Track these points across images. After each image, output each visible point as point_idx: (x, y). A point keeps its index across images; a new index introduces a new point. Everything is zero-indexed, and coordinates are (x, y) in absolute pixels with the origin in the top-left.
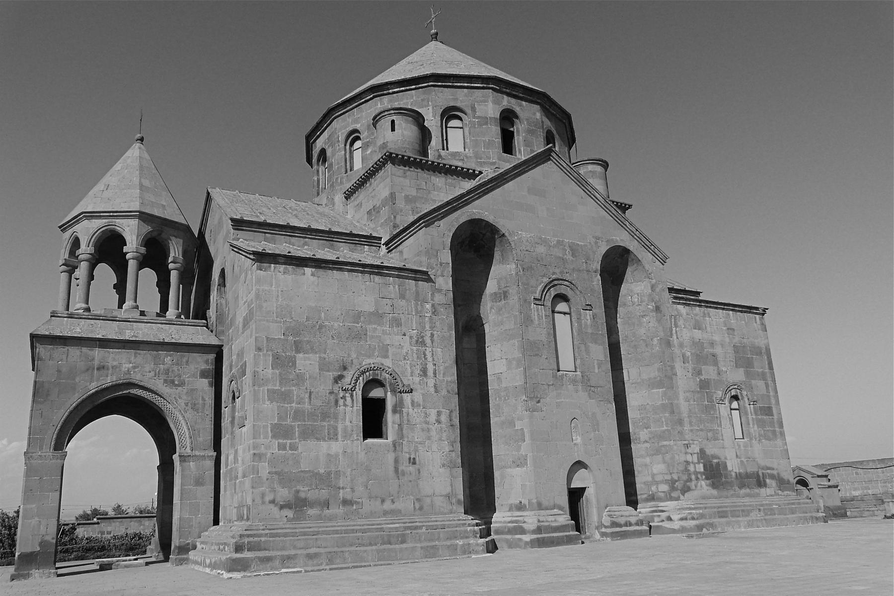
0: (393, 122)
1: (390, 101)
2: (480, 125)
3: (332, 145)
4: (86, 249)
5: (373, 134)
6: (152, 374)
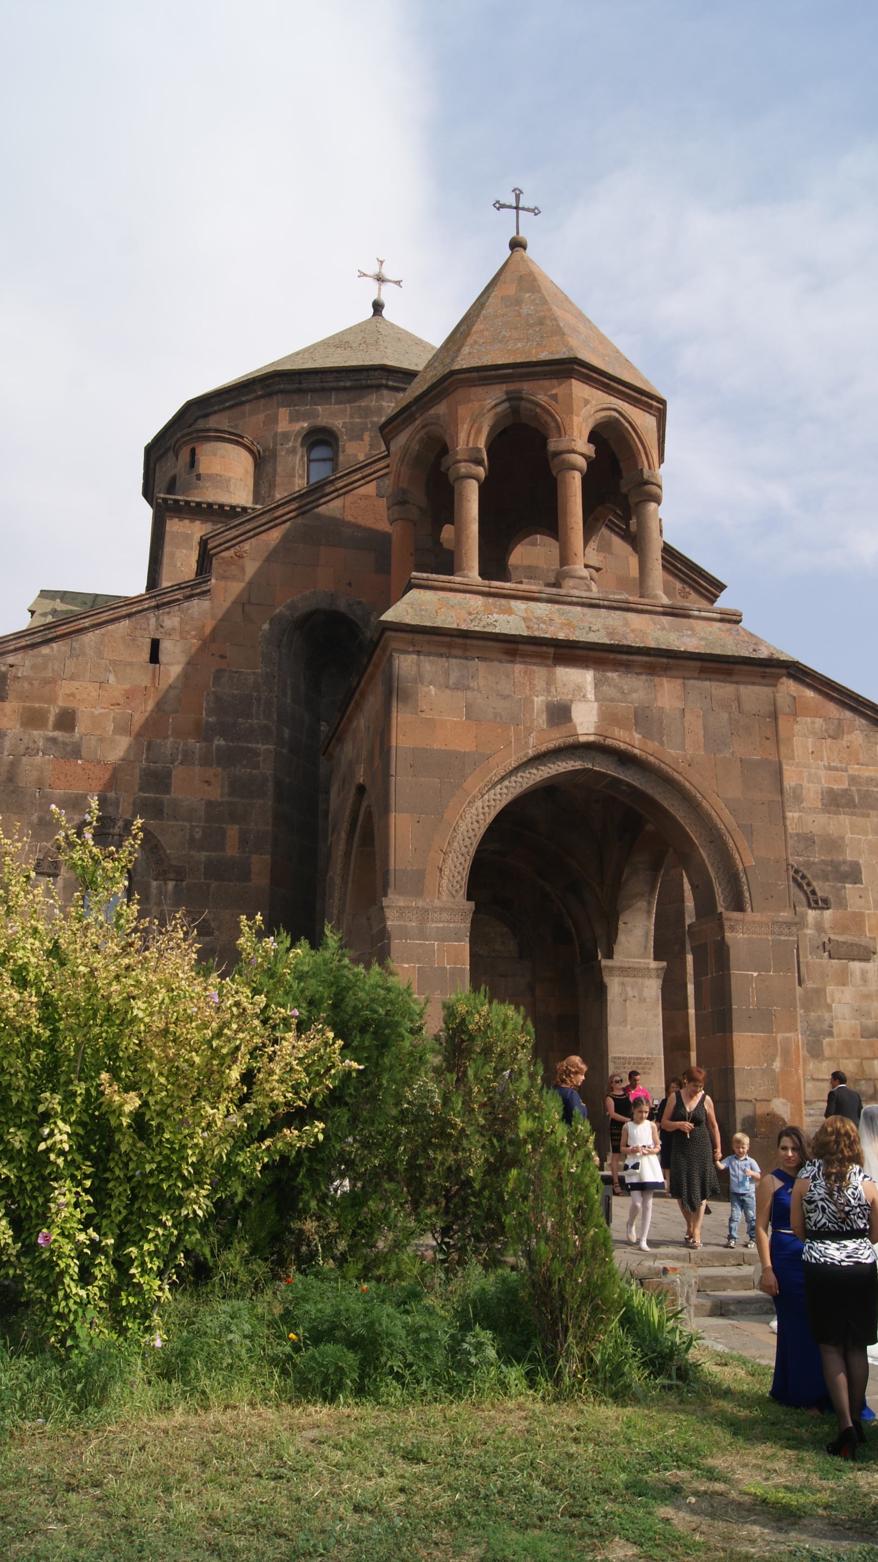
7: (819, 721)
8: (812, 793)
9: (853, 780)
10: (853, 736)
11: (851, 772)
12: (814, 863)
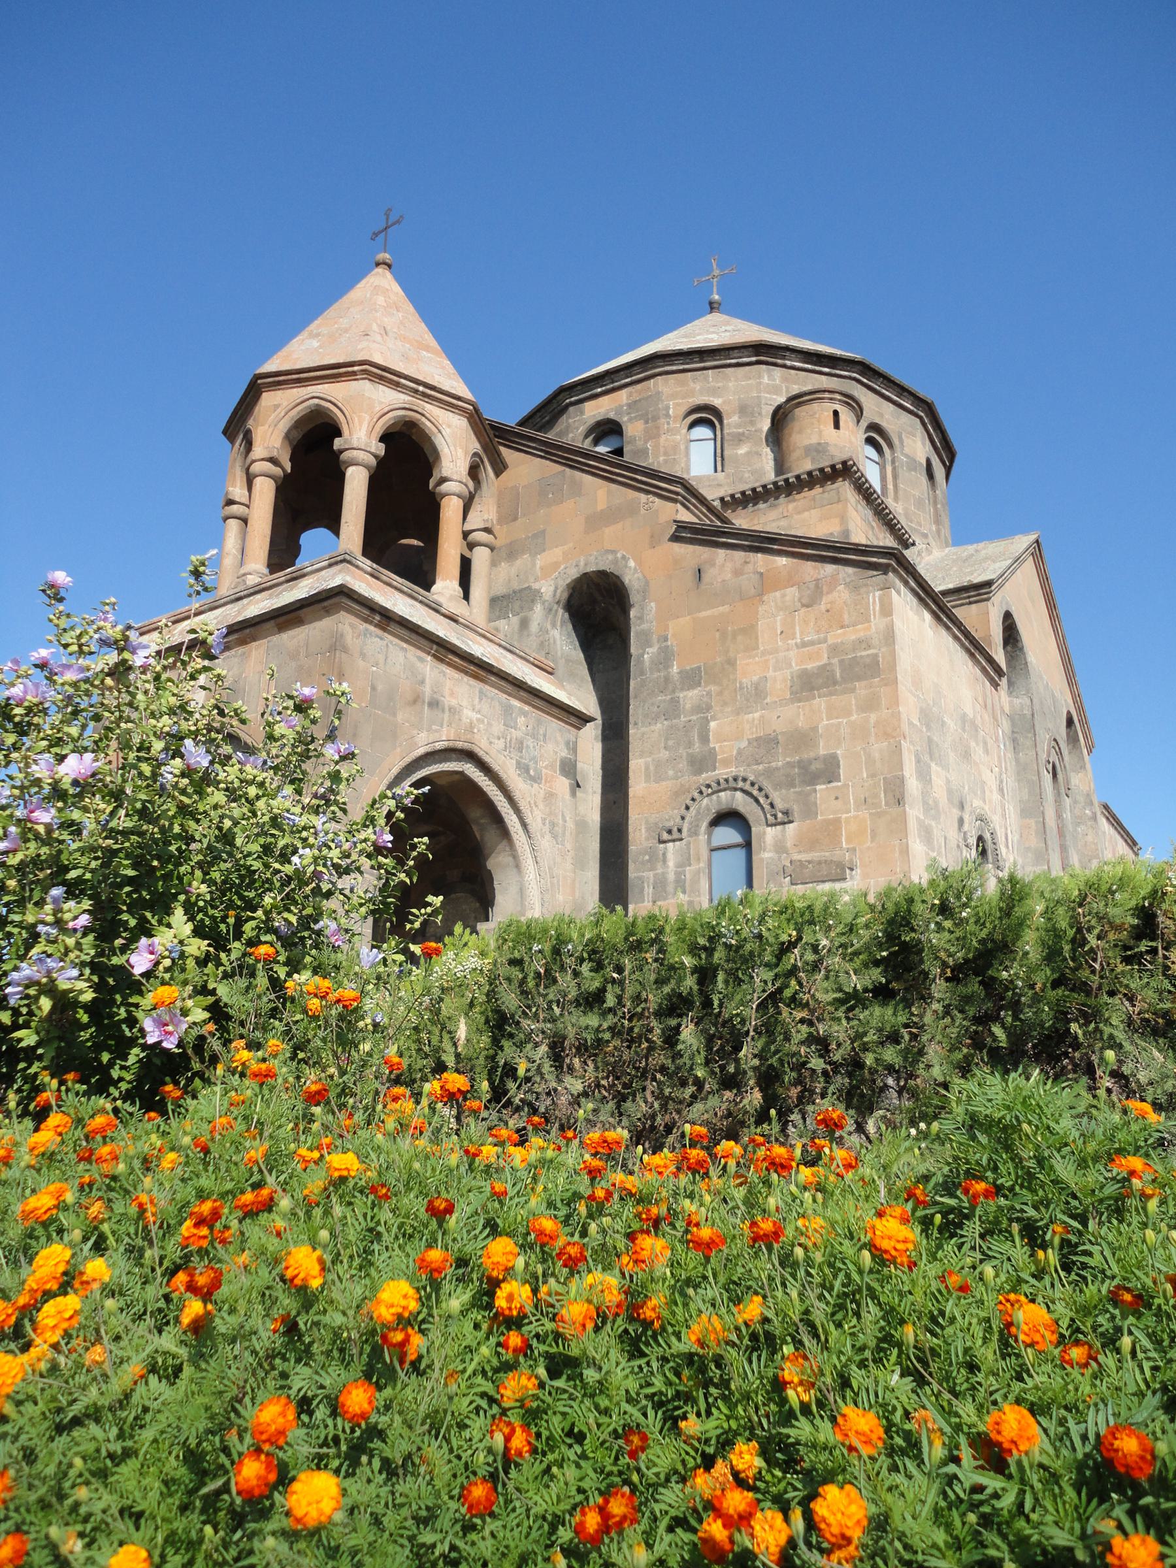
0: (836, 413)
1: (785, 379)
2: (910, 469)
3: (651, 419)
4: (361, 441)
5: (752, 423)
6: (500, 744)
7: (792, 593)
8: (779, 681)
9: (834, 650)
10: (835, 594)
11: (830, 641)
12: (777, 769)
